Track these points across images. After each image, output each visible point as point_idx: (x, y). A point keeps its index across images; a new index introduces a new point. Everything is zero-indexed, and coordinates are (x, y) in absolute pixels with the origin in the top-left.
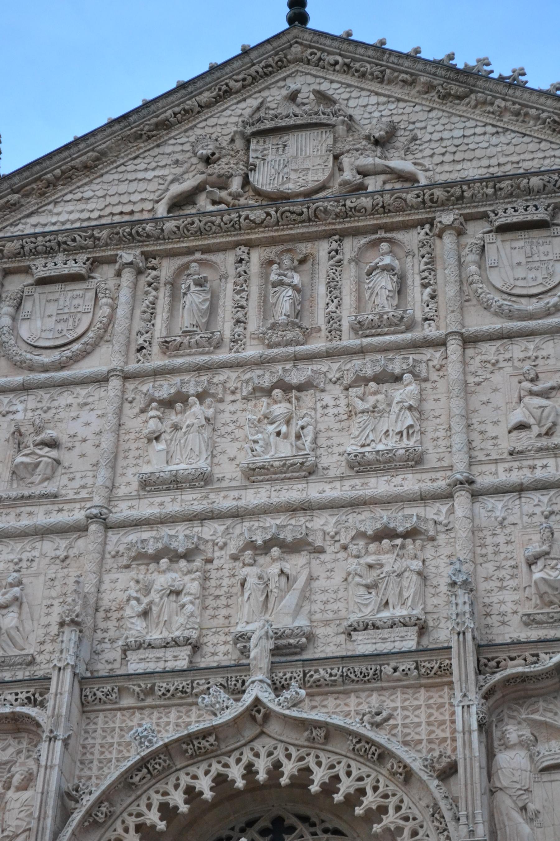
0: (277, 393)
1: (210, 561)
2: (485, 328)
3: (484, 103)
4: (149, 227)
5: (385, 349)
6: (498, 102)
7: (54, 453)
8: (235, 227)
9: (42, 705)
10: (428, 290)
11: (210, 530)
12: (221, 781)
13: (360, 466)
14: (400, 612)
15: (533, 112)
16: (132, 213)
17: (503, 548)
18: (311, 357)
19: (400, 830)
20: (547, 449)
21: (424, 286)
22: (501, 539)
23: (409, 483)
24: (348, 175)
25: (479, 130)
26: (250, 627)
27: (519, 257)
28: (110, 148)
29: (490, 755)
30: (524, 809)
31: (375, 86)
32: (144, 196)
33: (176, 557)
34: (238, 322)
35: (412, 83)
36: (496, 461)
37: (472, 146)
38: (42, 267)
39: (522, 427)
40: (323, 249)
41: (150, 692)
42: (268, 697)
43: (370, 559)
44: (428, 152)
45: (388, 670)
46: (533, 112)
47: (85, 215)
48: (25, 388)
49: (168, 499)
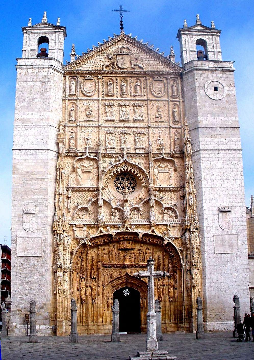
0: (124, 106)
1: (116, 134)
2: (153, 99)
3: (153, 55)
4: (103, 72)
7: (92, 113)
8: (116, 74)
10: (145, 90)
14: (142, 147)
16: (99, 67)
17: (155, 137)
18: (128, 100)
19: (143, 179)
20: (161, 121)
21: (144, 89)
22: (154, 136)
23: (142, 125)
24: (133, 66)
27: (157, 86)
28: (95, 54)
29: (153, 169)
30: (157, 177)
34: (117, 92)
36: (154, 122)
37: (151, 63)
38: (87, 77)
39: (157, 117)
40: (129, 79)
41: (111, 156)
42: (127, 159)
43: (138, 137)
44: (144, 62)
47: (92, 66)
48: (86, 100)
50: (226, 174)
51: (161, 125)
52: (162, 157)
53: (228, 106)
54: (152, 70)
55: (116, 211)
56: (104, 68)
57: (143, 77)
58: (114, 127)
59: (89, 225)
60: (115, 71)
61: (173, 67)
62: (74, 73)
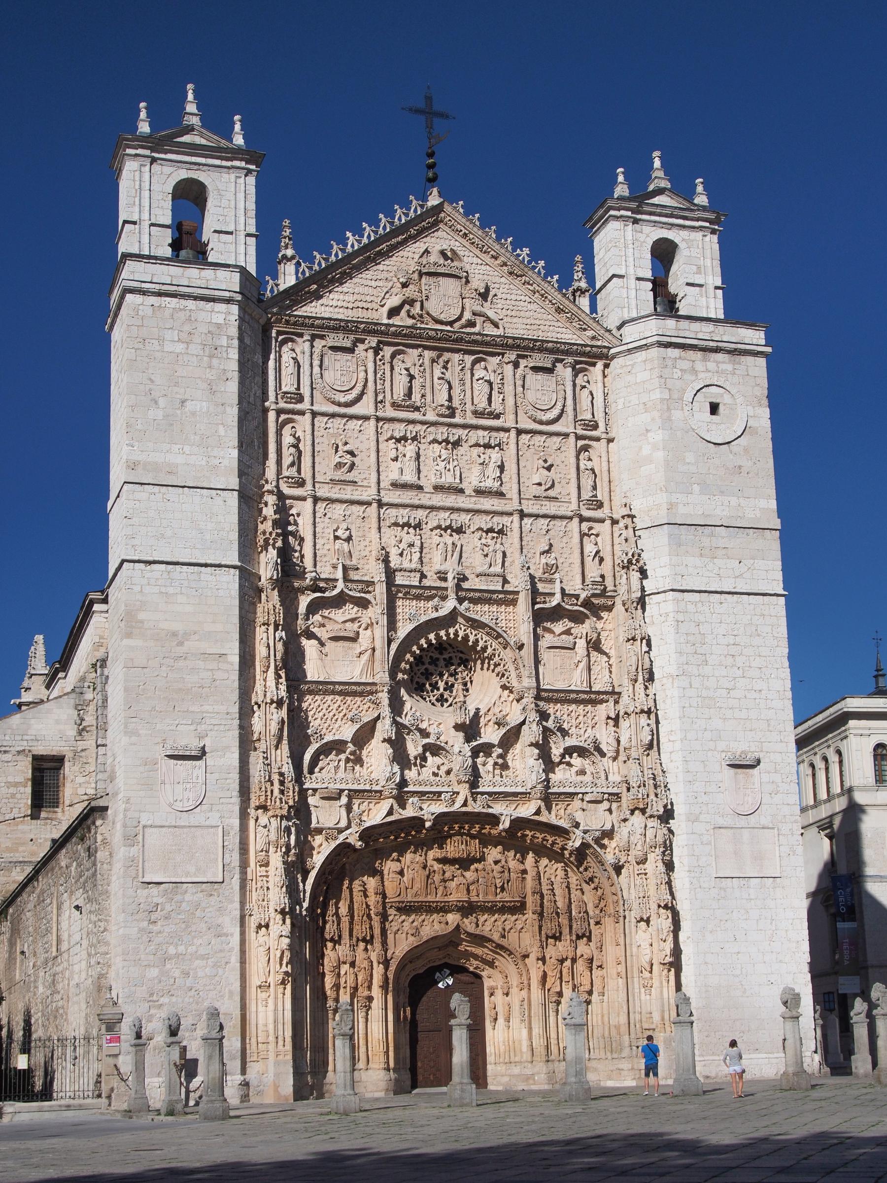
3: (528, 283)
5: (484, 428)
6: (534, 285)
8: (420, 337)
9: (369, 592)
10: (502, 396)
11: (421, 514)
12: (438, 637)
13: (479, 492)
15: (549, 297)
25: (523, 298)
26: (442, 568)
31: (478, 252)
32: (372, 298)
33: (409, 526)
34: (423, 396)
35: (496, 258)
39: (540, 484)
40: (456, 357)
44: (500, 306)
45: (495, 596)
46: (549, 297)
47: (345, 304)
48: (333, 416)
49: (401, 493)
50: (740, 661)
51: (548, 507)
52: (554, 604)
53: (747, 464)
54: (522, 332)
55: (428, 754)
56: (385, 315)
57: (498, 354)
58: (418, 507)
59: (356, 791)
60: (420, 329)
61: (585, 330)
62: (295, 324)
